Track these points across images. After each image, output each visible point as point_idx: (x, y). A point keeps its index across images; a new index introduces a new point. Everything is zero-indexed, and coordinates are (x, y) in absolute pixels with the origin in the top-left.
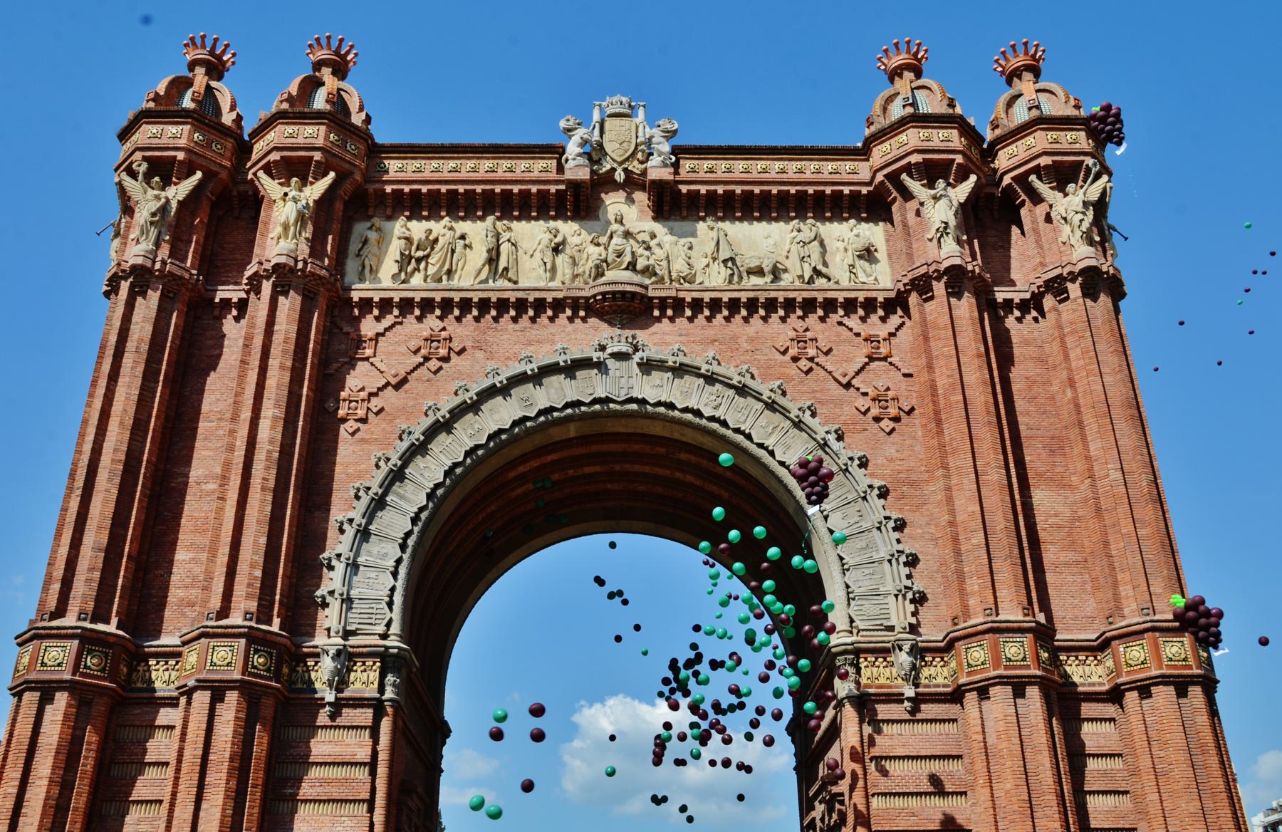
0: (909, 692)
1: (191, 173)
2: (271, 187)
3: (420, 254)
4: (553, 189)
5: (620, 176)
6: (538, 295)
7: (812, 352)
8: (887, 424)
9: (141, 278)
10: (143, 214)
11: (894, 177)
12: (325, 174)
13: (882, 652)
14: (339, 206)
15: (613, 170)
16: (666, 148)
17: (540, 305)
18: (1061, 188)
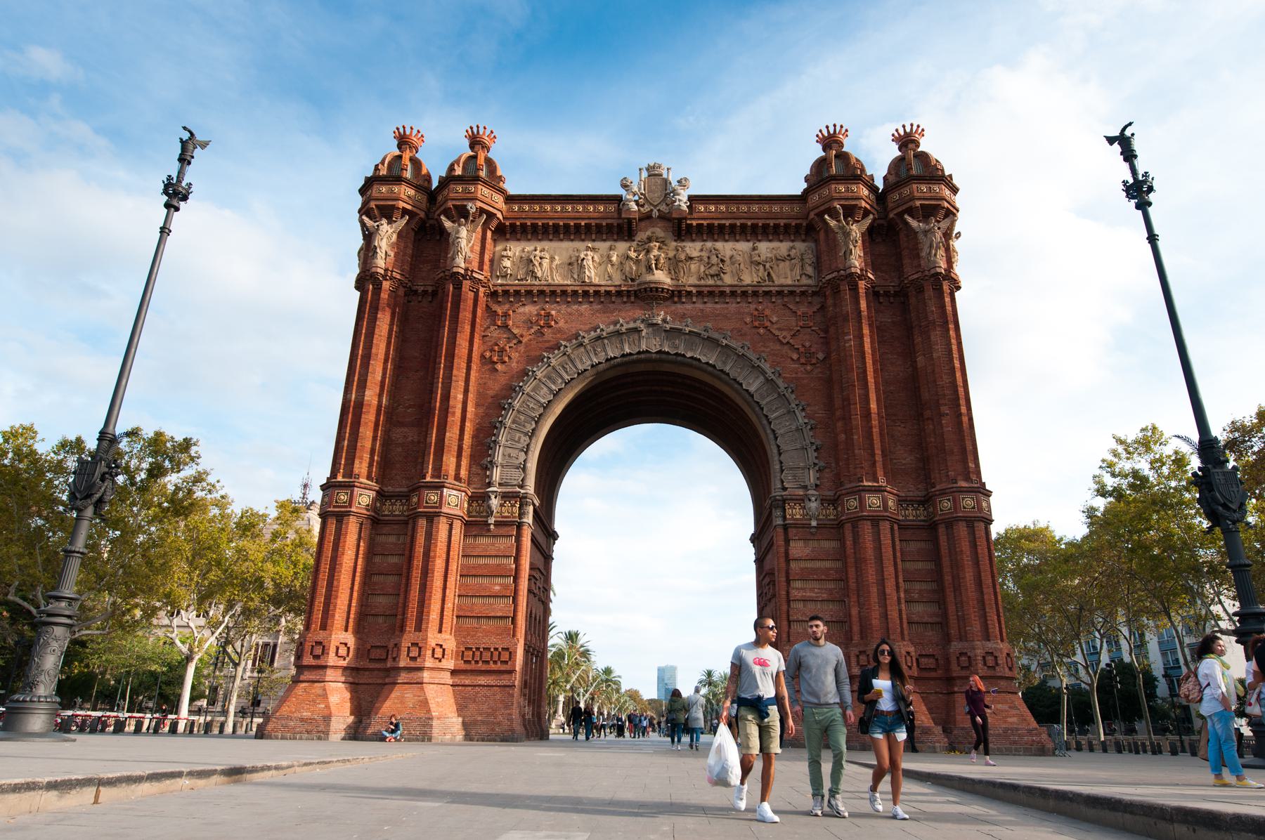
0: (814, 523)
2: (448, 224)
4: (615, 222)
5: (655, 213)
7: (768, 324)
8: (809, 368)
13: (801, 500)
14: (489, 234)
16: (683, 196)
17: (608, 293)
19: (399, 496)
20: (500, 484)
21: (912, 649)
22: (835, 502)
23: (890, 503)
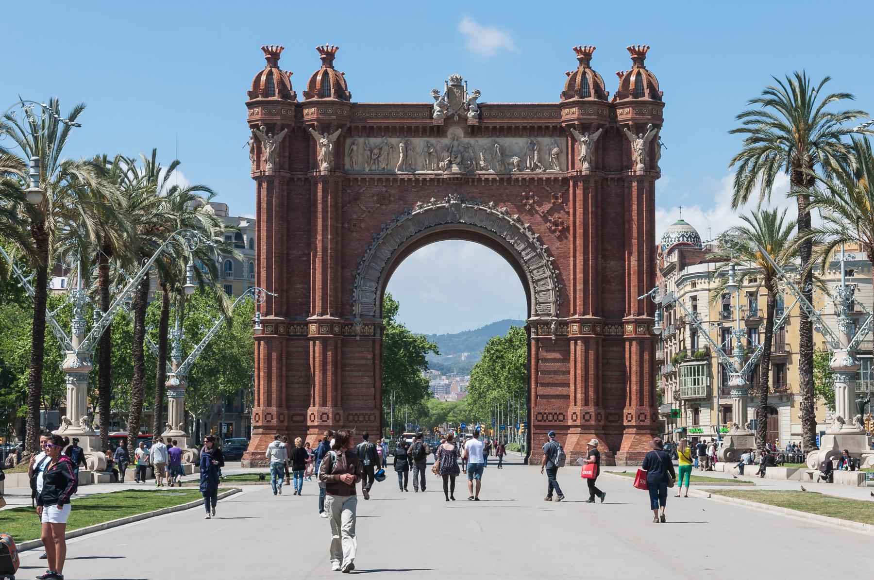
1: (283, 129)
2: (315, 134)
3: (374, 157)
5: (456, 118)
6: (423, 177)
9: (270, 180)
10: (267, 152)
11: (569, 126)
12: (337, 129)
14: (342, 138)
15: (453, 115)
17: (425, 179)
18: (637, 135)
19: (298, 325)
20: (361, 316)
21: (602, 412)
22: (567, 324)
23: (598, 329)
